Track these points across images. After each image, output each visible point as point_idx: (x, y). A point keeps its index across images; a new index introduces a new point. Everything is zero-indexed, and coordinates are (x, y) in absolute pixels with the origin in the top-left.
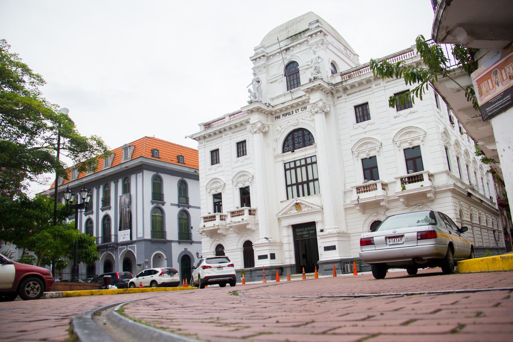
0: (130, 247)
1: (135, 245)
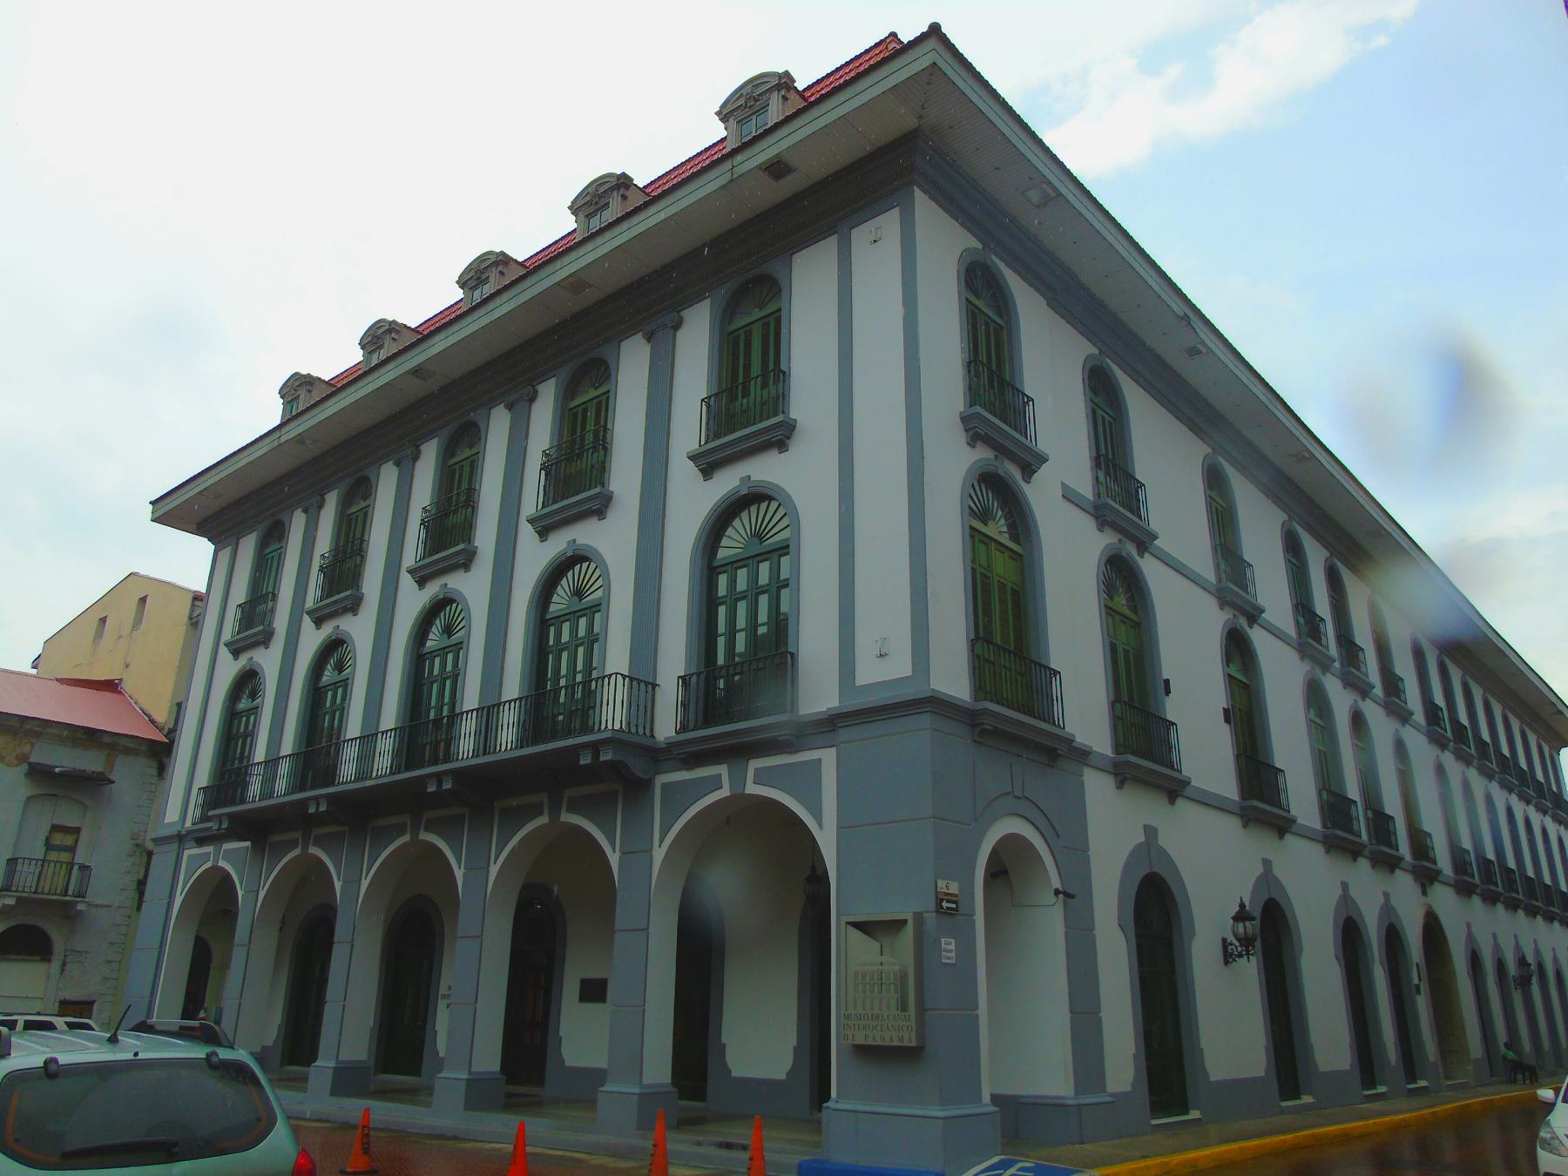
0: (762, 777)
1: (828, 758)
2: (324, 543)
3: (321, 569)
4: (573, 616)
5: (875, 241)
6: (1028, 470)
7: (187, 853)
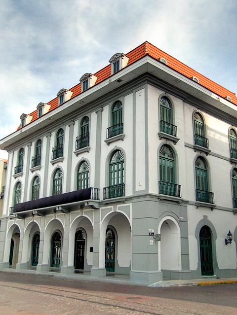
1: (131, 205)
2: (33, 154)
3: (32, 160)
4: (84, 173)
6: (175, 142)
7: (8, 221)
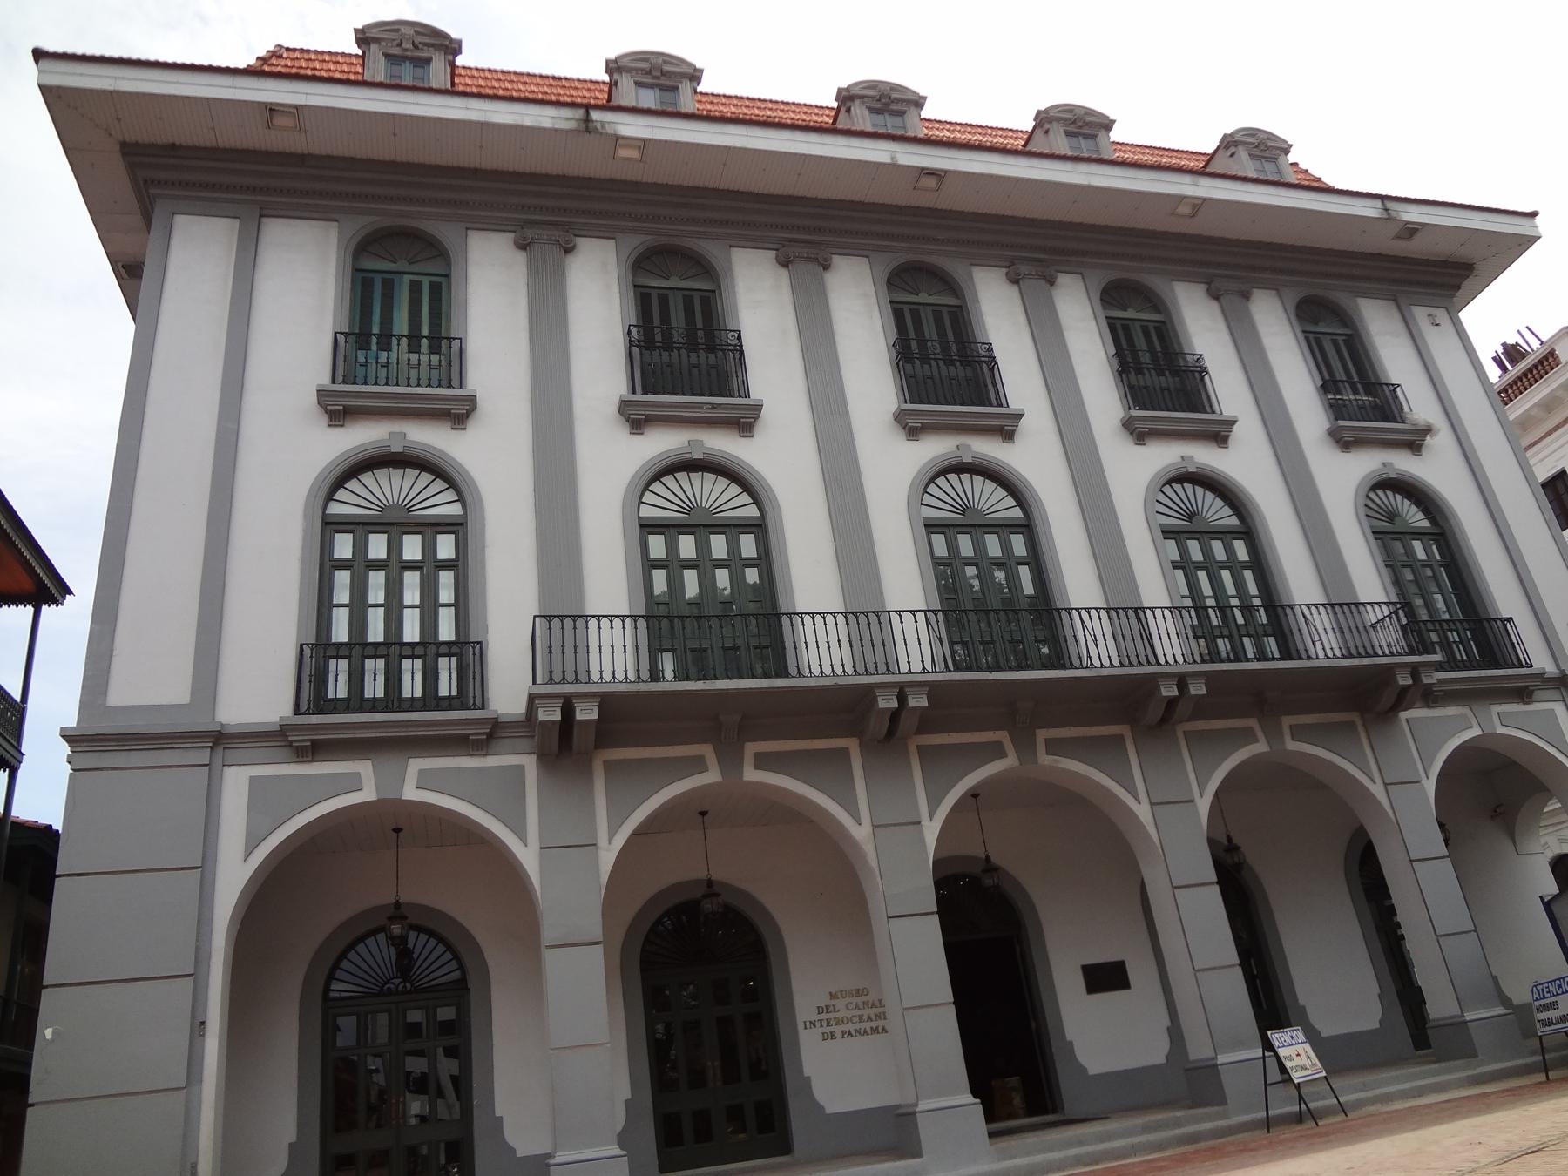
5: (1437, 325)
